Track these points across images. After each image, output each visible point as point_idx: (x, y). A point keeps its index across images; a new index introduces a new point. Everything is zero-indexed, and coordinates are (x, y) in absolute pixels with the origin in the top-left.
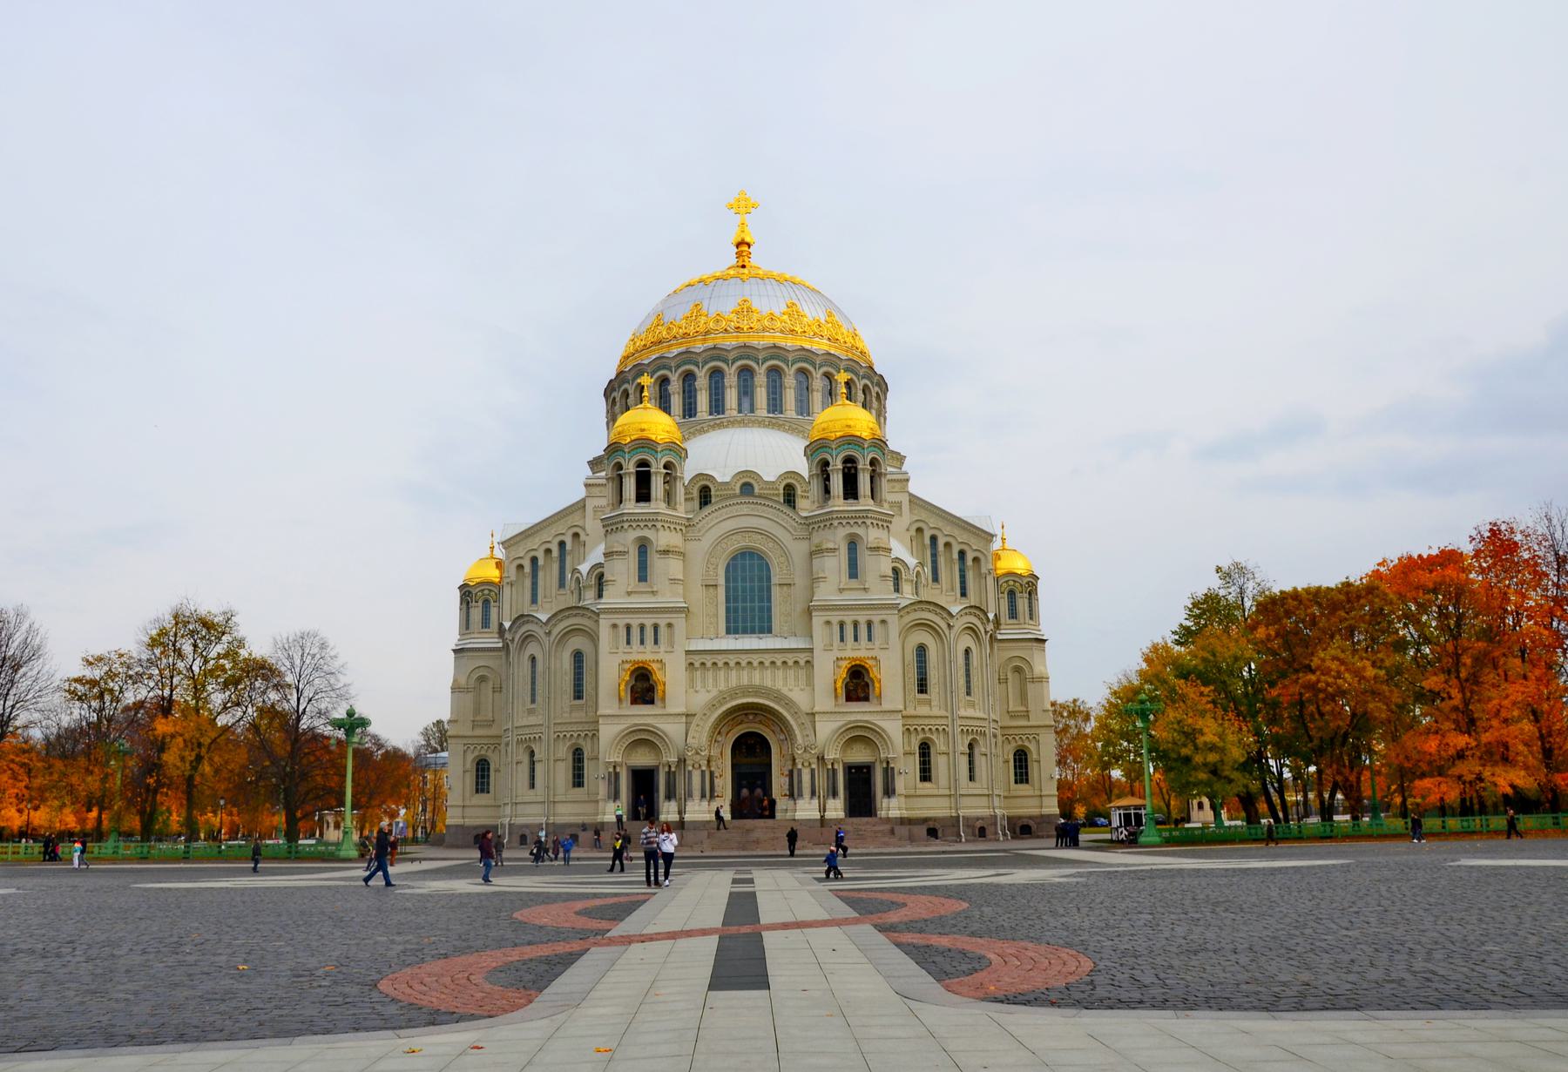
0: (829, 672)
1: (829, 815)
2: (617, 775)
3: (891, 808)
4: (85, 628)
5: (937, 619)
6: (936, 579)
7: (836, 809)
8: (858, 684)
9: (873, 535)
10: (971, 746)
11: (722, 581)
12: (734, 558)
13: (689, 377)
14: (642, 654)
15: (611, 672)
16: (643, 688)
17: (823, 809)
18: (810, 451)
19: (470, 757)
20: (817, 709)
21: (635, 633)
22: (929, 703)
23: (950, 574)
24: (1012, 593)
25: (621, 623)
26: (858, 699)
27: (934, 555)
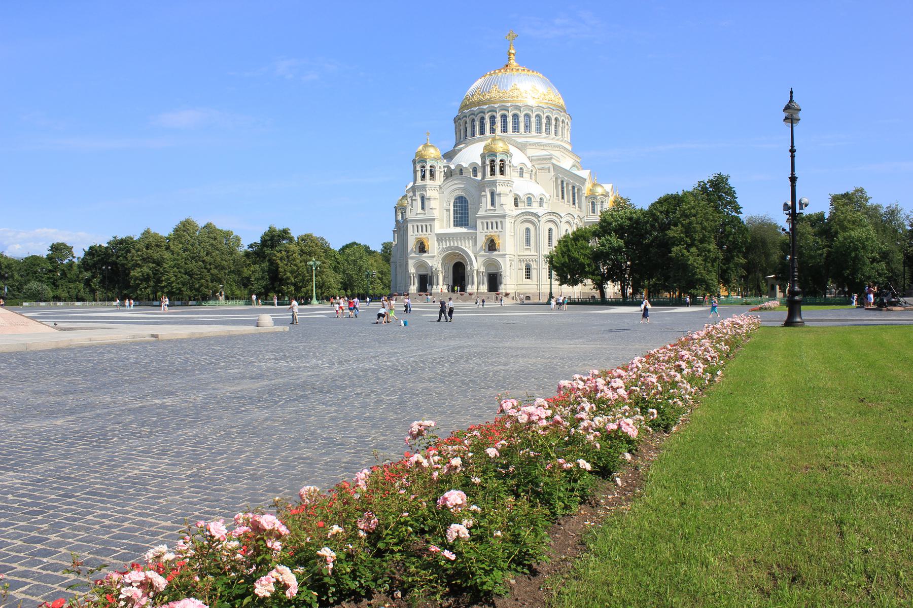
0: (482, 241)
3: (502, 289)
4: (249, 236)
6: (563, 198)
7: (484, 288)
8: (492, 246)
9: (499, 189)
11: (452, 207)
13: (473, 120)
14: (422, 235)
15: (412, 243)
16: (422, 248)
18: (483, 156)
22: (530, 250)
23: (568, 196)
24: (593, 203)
27: (563, 188)
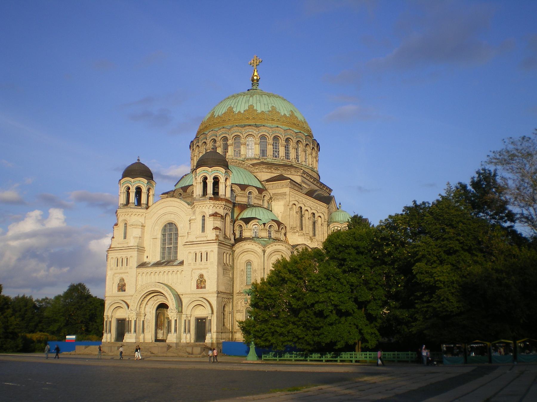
1: (183, 341)
11: (159, 236)
12: (166, 226)
21: (120, 261)
26: (201, 288)
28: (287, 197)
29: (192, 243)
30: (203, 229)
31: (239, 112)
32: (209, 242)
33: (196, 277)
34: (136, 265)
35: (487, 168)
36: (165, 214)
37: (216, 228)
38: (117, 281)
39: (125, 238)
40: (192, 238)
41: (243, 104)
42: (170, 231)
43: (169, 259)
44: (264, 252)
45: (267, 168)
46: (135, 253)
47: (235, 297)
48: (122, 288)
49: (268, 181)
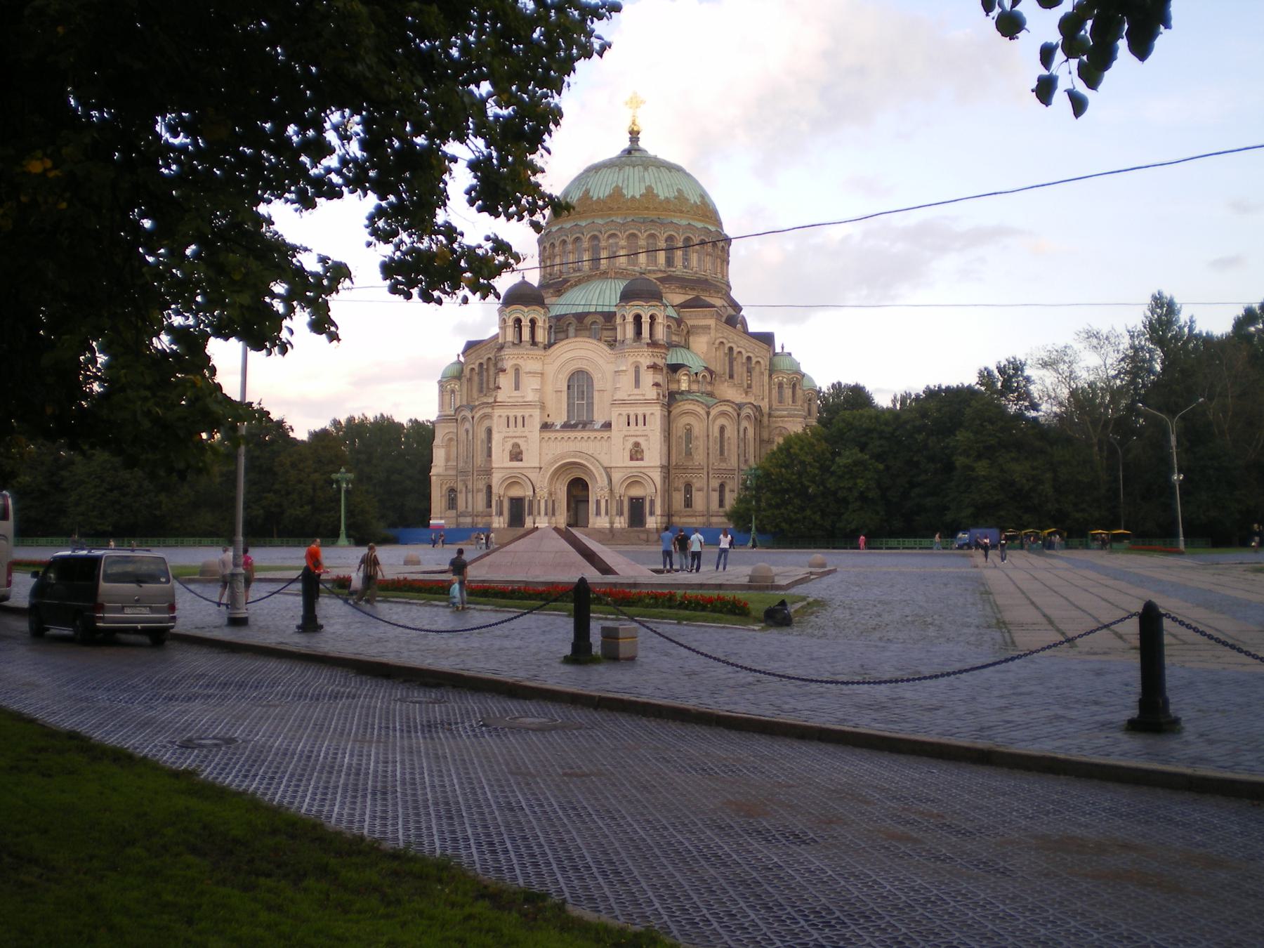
1: (617, 525)
2: (501, 502)
5: (699, 409)
7: (621, 523)
10: (722, 486)
17: (612, 523)
19: (445, 488)
20: (613, 465)
25: (504, 415)
28: (713, 332)
29: (623, 403)
30: (637, 383)
31: (633, 197)
32: (647, 403)
33: (629, 445)
34: (538, 427)
35: (1027, 372)
36: (573, 359)
37: (657, 385)
38: (509, 446)
39: (517, 388)
40: (620, 395)
41: (637, 184)
42: (580, 383)
43: (578, 423)
44: (708, 414)
45: (682, 287)
46: (536, 412)
47: (673, 471)
48: (516, 455)
49: (684, 305)
